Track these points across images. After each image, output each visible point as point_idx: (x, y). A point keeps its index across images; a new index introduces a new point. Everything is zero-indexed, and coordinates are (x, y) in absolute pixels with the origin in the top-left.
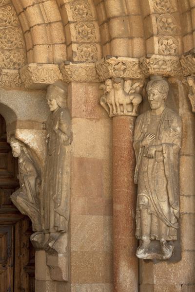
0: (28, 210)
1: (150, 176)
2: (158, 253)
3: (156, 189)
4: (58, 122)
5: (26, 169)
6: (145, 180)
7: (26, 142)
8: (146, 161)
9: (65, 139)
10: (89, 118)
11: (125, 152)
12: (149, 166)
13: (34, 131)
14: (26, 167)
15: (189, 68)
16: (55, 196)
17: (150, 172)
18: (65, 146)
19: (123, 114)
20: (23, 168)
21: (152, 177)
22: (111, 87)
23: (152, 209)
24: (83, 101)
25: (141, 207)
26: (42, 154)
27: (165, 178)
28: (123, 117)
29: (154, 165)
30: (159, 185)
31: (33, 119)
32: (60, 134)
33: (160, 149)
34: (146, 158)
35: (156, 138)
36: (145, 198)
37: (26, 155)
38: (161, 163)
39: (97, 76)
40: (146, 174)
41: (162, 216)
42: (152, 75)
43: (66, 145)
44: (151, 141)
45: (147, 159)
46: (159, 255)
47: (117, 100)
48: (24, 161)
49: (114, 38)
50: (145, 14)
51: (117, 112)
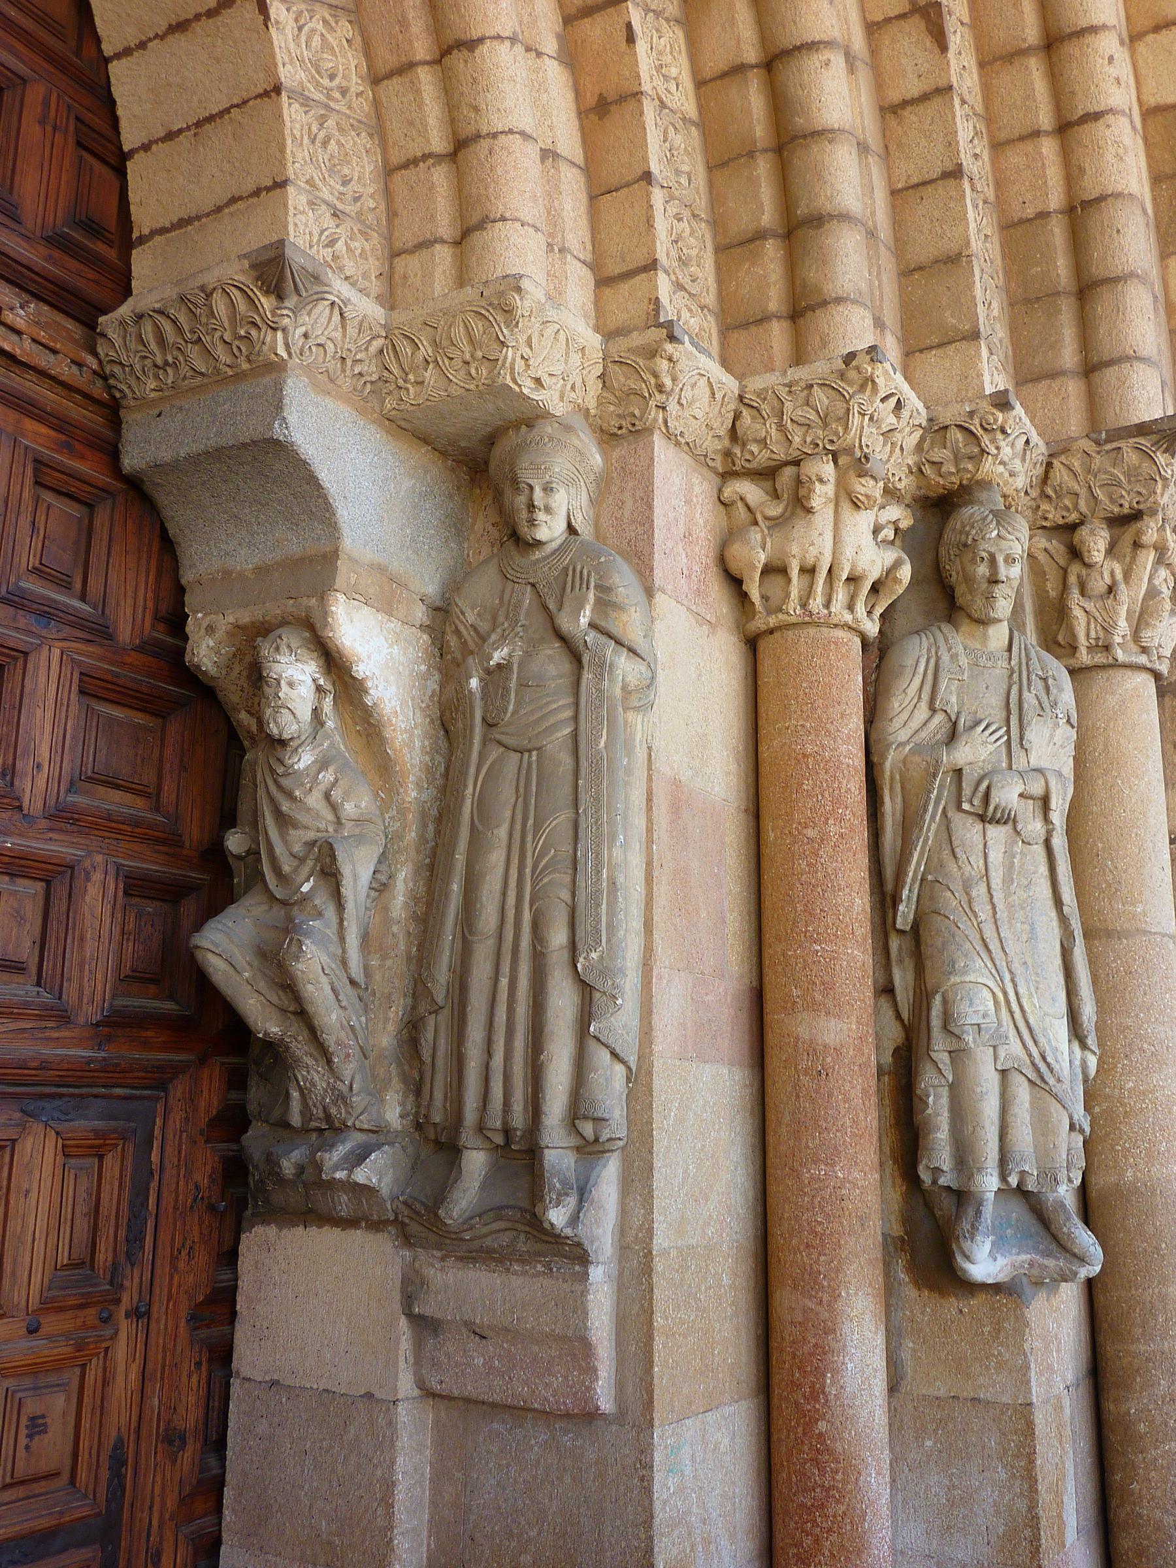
0: (334, 1017)
1: (998, 896)
2: (1048, 1254)
3: (1029, 961)
4: (591, 596)
5: (334, 807)
6: (982, 916)
7: (361, 670)
8: (969, 832)
9: (632, 680)
10: (694, 608)
11: (851, 785)
12: (992, 857)
13: (394, 625)
14: (336, 795)
15: (1098, 492)
16: (594, 955)
17: (996, 882)
18: (631, 716)
19: (848, 617)
20: (315, 800)
21: (1010, 907)
22: (830, 489)
23: (1015, 1047)
24: (682, 529)
25: (969, 1038)
26: (409, 745)
27: (1053, 914)
28: (840, 633)
29: (1009, 854)
30: (1041, 945)
31: (395, 567)
32: (609, 653)
33: (1037, 789)
34: (970, 820)
35: (1009, 741)
37: (327, 736)
38: (1039, 850)
39: (727, 442)
40: (983, 888)
41: (1059, 1081)
42: (985, 484)
43: (636, 709)
44: (991, 748)
45: (979, 826)
46: (1050, 1263)
47: (848, 552)
48: (323, 764)
49: (839, 300)
50: (924, 249)
51: (827, 605)
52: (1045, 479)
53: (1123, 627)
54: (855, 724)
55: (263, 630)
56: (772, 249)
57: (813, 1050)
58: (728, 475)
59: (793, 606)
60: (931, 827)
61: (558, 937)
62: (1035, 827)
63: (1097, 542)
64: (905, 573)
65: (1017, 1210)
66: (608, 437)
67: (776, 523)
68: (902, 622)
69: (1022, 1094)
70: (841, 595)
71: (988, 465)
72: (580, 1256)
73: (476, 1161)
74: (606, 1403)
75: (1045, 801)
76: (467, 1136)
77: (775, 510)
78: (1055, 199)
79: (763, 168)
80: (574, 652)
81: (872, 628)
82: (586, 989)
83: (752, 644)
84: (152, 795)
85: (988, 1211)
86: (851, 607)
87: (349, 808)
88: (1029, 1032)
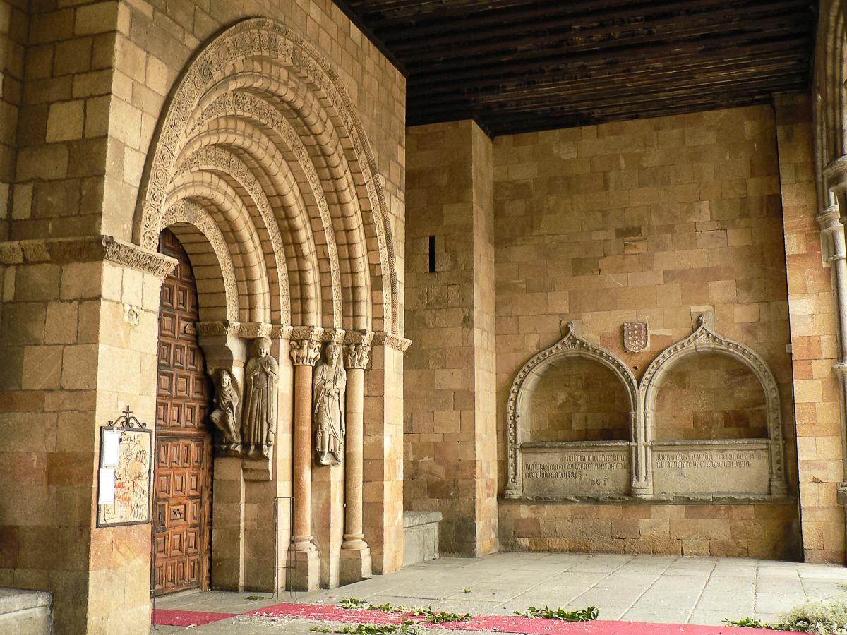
8: (326, 399)
17: (330, 405)
33: (337, 392)
36: (326, 425)
48: (230, 390)
52: (345, 337)
53: (357, 362)
54: (311, 380)
55: (222, 370)
56: (299, 301)
57: (301, 431)
58: (291, 341)
59: (301, 362)
60: (321, 397)
61: (265, 417)
62: (337, 398)
63: (353, 348)
64: (319, 357)
65: (330, 454)
66: (272, 338)
67: (298, 349)
68: (319, 363)
69: (332, 437)
70: (308, 361)
71: (333, 339)
72: (268, 459)
73: (253, 447)
74: (271, 478)
75: (339, 394)
76: (252, 444)
77: (298, 347)
78: (350, 285)
79: (298, 287)
80: (267, 375)
81: (314, 365)
82: (269, 424)
83: (294, 368)
84: (202, 394)
85: (325, 455)
86: (310, 362)
87: (233, 397)
88: (333, 429)
